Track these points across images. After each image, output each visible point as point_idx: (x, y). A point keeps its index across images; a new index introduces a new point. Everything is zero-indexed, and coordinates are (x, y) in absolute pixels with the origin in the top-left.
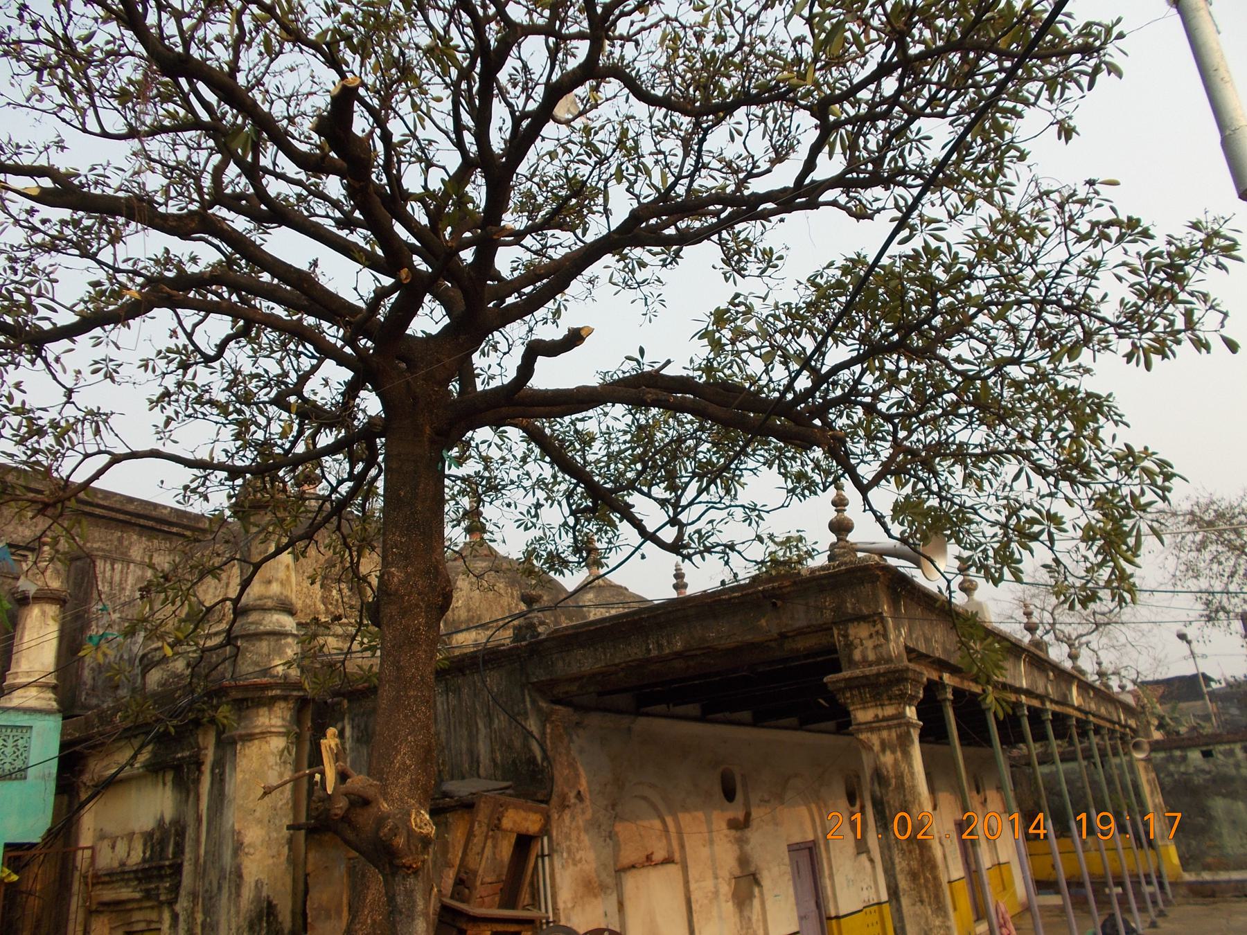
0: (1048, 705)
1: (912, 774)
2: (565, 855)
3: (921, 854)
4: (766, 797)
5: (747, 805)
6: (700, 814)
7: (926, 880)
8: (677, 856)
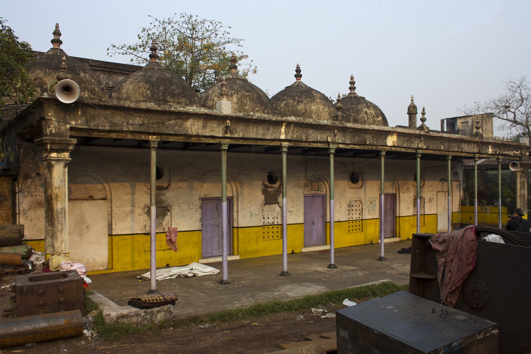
0: (331, 146)
1: (51, 178)
2: (26, 193)
3: (48, 206)
4: (186, 178)
5: (170, 181)
6: (128, 184)
7: (48, 214)
8: (109, 197)
